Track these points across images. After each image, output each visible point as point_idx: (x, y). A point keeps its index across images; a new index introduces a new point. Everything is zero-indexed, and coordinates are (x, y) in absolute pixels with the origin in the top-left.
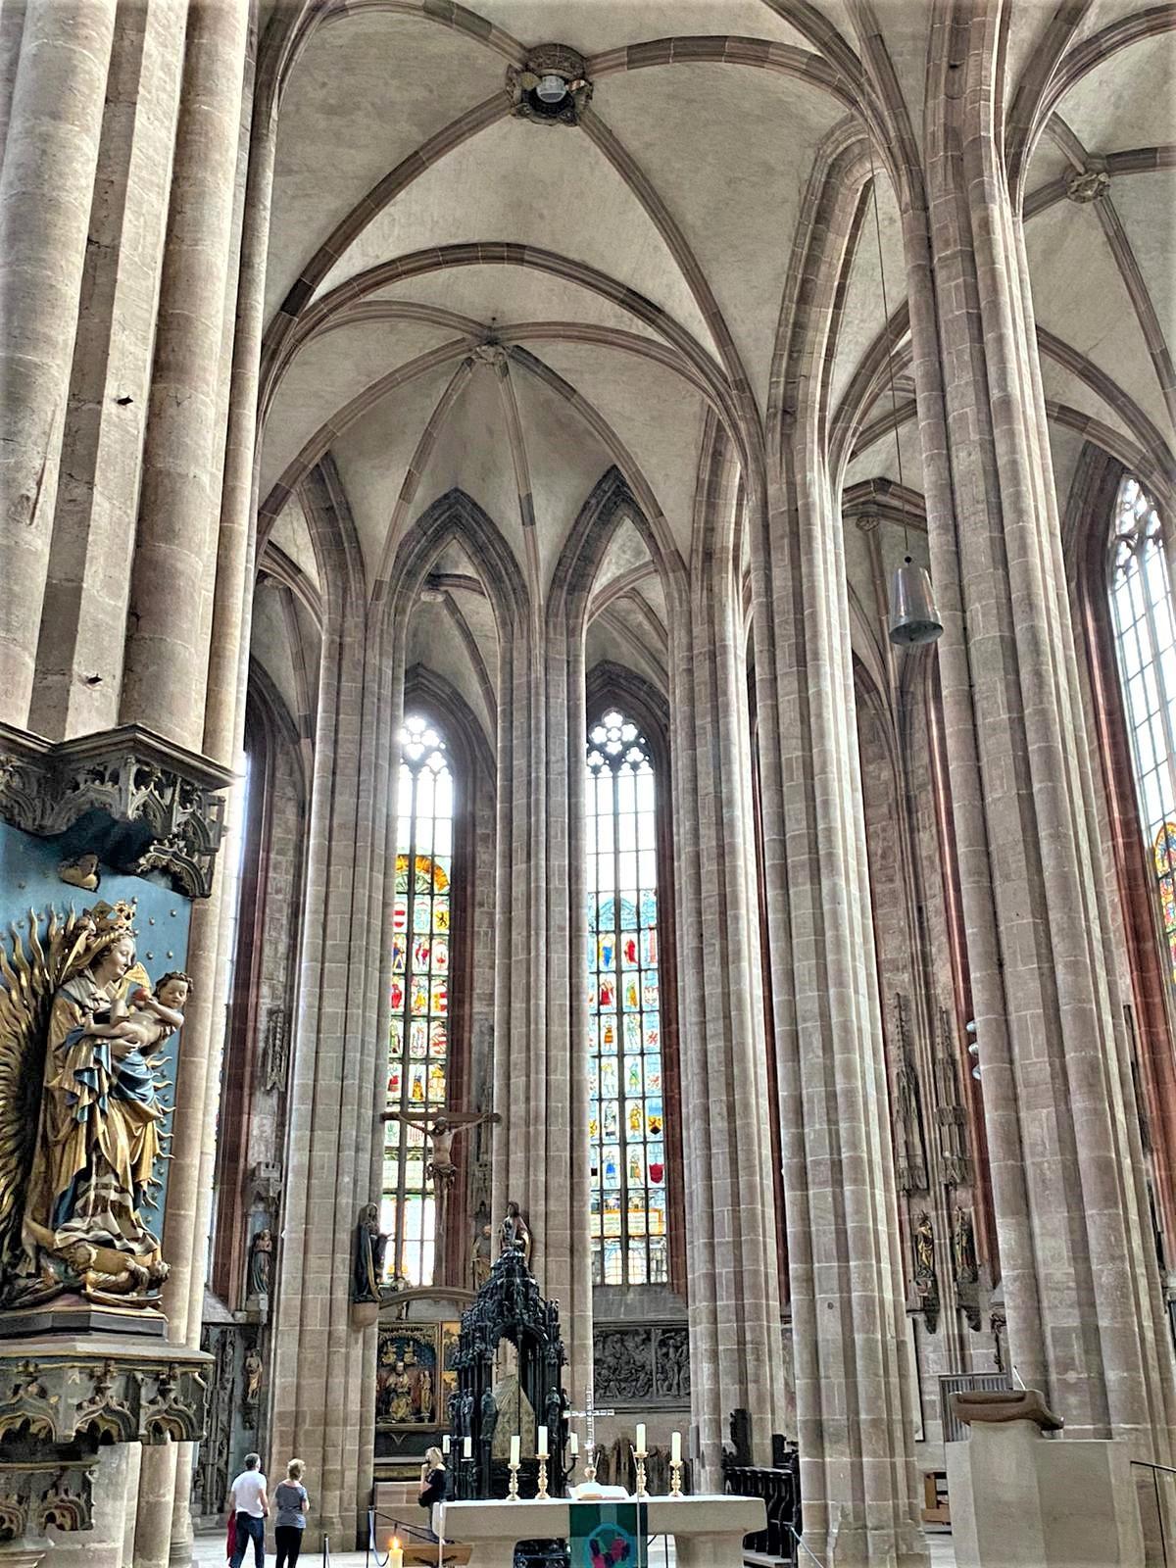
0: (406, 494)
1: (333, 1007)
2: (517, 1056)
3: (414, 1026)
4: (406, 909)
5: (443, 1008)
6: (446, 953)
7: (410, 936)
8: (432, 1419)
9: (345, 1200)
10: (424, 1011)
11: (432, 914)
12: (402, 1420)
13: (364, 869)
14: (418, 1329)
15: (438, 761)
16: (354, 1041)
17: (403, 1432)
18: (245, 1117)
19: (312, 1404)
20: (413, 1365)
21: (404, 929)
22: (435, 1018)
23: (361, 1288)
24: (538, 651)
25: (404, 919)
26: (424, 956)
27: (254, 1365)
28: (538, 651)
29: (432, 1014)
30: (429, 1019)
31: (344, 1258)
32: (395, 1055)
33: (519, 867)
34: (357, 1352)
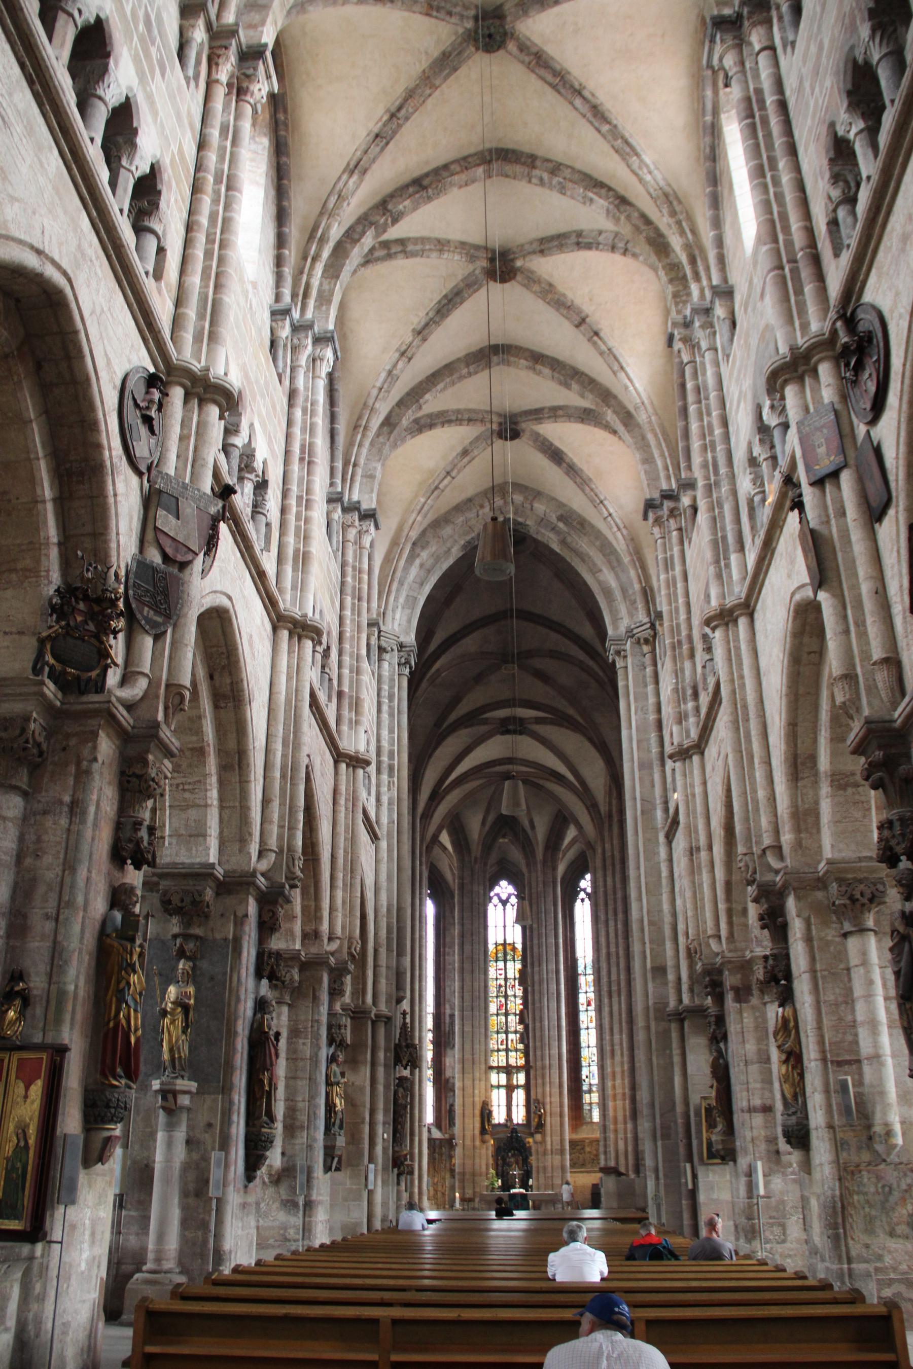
0: (483, 823)
1: (467, 1029)
2: (538, 1044)
7: (506, 979)
9: (477, 1099)
11: (514, 968)
13: (476, 974)
15: (514, 900)
16: (476, 1041)
19: (468, 1169)
23: (483, 1131)
24: (540, 879)
28: (540, 879)
31: (478, 1119)
33: (536, 969)
34: (484, 1151)
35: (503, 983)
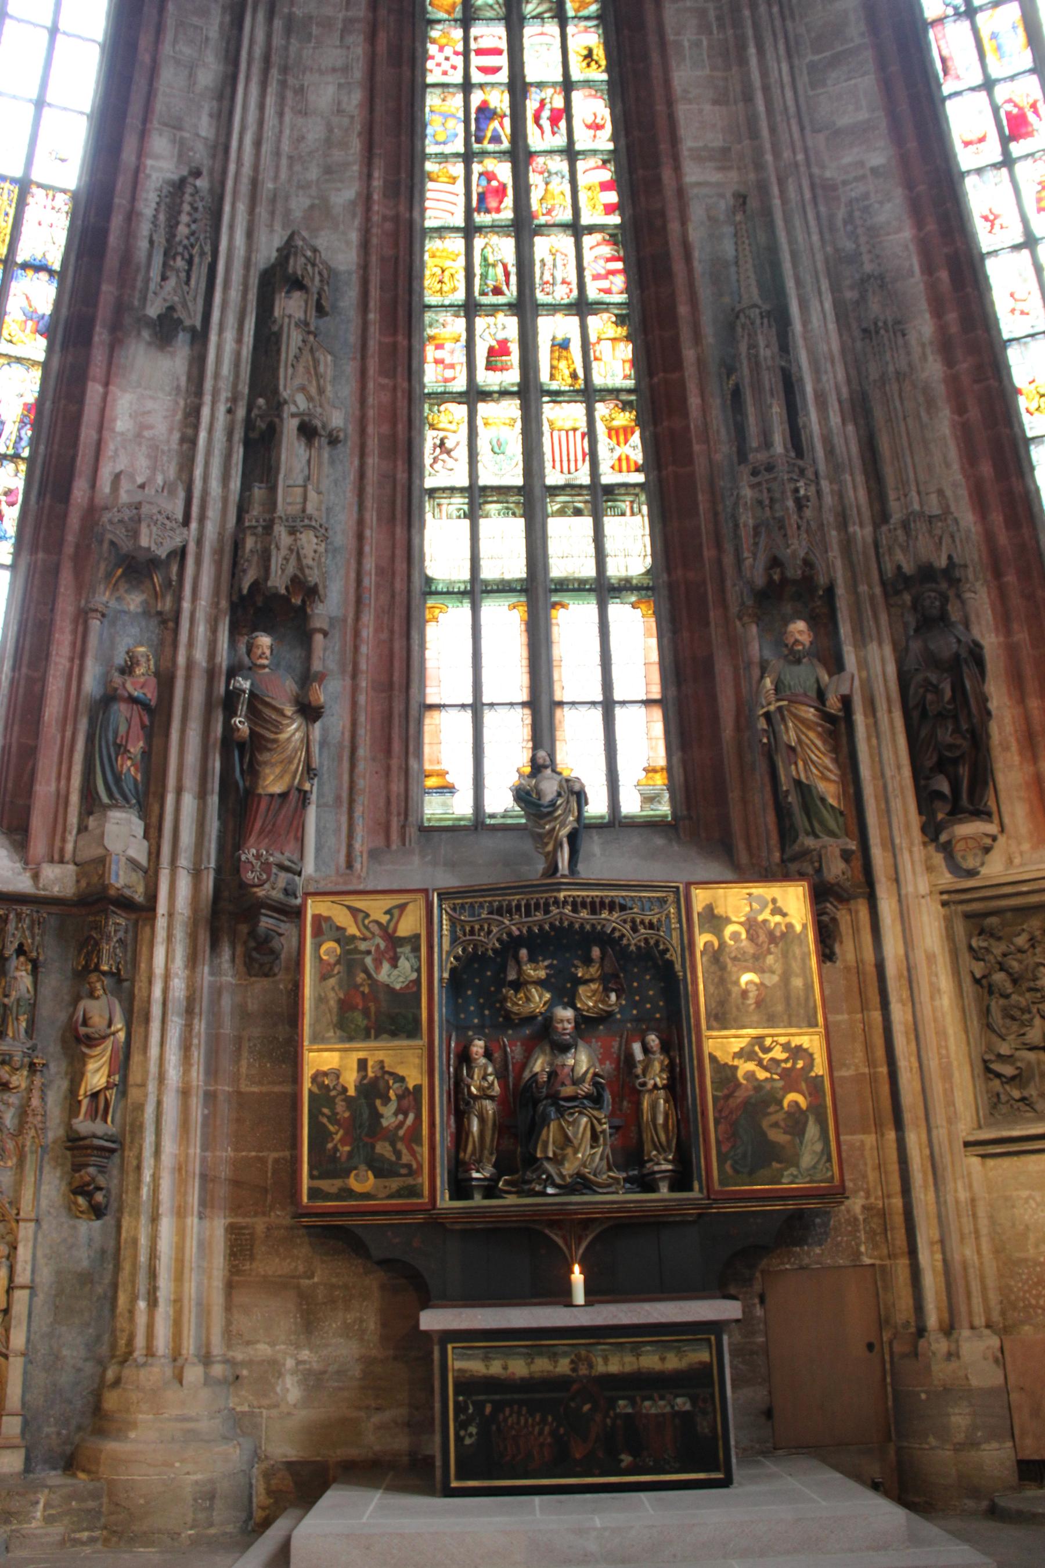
3: (542, 246)
4: (503, 45)
5: (609, 209)
6: (606, 113)
8: (681, 1181)
10: (567, 216)
12: (582, 1183)
14: (612, 906)
17: (586, 1224)
18: (94, 390)
20: (605, 1018)
21: (503, 76)
22: (591, 229)
25: (503, 61)
26: (554, 120)
27: (98, 1021)
29: (585, 220)
30: (576, 229)
32: (501, 300)
35: (500, 101)
